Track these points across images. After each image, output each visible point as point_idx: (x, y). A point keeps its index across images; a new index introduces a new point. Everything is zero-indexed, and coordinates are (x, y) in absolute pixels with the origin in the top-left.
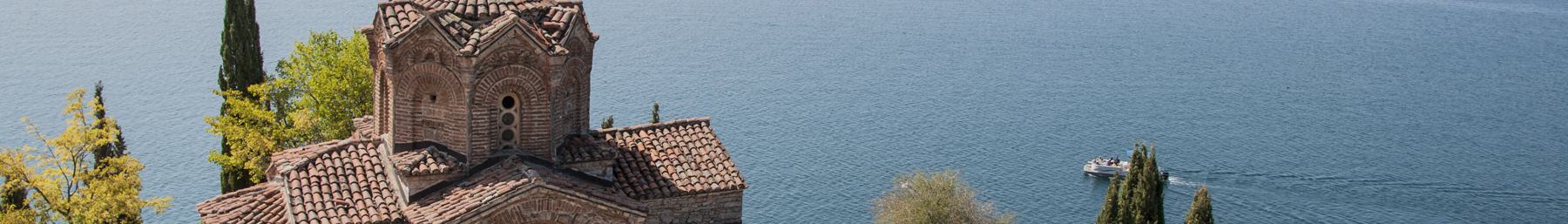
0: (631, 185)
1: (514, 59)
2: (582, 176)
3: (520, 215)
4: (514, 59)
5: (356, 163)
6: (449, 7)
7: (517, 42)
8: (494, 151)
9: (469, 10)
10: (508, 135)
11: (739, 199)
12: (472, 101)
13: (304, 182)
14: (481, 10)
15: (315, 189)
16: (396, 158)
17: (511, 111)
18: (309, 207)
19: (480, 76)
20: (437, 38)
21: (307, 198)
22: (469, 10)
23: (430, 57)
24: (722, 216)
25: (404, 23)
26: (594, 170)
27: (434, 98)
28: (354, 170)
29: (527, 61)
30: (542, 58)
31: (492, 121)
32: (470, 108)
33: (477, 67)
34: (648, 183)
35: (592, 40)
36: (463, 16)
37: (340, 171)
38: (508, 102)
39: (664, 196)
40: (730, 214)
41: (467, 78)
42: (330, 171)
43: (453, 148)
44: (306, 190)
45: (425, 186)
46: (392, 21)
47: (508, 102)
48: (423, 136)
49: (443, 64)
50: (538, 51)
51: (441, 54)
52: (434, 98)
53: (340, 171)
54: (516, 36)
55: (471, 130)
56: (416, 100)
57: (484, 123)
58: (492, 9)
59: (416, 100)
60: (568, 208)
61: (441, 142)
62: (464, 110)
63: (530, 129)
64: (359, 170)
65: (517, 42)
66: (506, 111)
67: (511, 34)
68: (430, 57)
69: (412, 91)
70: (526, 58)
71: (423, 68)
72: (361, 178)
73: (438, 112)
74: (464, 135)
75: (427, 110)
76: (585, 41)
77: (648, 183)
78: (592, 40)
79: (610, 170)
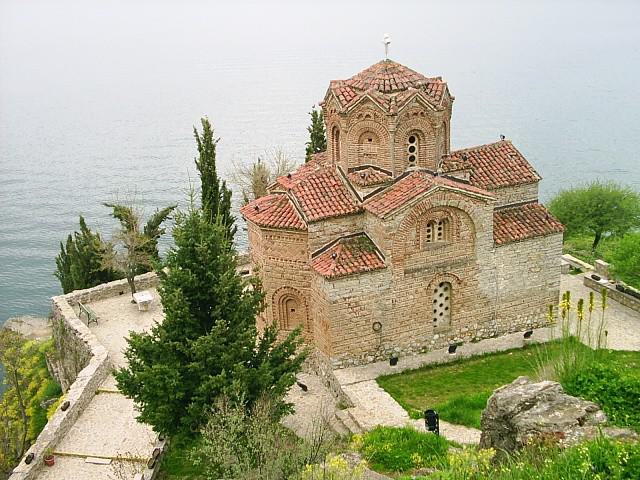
1: (416, 114)
6: (376, 87)
9: (387, 88)
10: (412, 159)
14: (394, 87)
17: (413, 145)
18: (311, 206)
22: (387, 88)
25: (349, 98)
26: (460, 176)
27: (370, 140)
36: (385, 92)
41: (392, 127)
42: (315, 185)
44: (305, 197)
45: (372, 191)
46: (342, 98)
47: (412, 140)
52: (370, 140)
56: (360, 142)
59: (360, 142)
62: (390, 147)
68: (368, 116)
74: (390, 160)
75: (367, 147)
79: (468, 175)
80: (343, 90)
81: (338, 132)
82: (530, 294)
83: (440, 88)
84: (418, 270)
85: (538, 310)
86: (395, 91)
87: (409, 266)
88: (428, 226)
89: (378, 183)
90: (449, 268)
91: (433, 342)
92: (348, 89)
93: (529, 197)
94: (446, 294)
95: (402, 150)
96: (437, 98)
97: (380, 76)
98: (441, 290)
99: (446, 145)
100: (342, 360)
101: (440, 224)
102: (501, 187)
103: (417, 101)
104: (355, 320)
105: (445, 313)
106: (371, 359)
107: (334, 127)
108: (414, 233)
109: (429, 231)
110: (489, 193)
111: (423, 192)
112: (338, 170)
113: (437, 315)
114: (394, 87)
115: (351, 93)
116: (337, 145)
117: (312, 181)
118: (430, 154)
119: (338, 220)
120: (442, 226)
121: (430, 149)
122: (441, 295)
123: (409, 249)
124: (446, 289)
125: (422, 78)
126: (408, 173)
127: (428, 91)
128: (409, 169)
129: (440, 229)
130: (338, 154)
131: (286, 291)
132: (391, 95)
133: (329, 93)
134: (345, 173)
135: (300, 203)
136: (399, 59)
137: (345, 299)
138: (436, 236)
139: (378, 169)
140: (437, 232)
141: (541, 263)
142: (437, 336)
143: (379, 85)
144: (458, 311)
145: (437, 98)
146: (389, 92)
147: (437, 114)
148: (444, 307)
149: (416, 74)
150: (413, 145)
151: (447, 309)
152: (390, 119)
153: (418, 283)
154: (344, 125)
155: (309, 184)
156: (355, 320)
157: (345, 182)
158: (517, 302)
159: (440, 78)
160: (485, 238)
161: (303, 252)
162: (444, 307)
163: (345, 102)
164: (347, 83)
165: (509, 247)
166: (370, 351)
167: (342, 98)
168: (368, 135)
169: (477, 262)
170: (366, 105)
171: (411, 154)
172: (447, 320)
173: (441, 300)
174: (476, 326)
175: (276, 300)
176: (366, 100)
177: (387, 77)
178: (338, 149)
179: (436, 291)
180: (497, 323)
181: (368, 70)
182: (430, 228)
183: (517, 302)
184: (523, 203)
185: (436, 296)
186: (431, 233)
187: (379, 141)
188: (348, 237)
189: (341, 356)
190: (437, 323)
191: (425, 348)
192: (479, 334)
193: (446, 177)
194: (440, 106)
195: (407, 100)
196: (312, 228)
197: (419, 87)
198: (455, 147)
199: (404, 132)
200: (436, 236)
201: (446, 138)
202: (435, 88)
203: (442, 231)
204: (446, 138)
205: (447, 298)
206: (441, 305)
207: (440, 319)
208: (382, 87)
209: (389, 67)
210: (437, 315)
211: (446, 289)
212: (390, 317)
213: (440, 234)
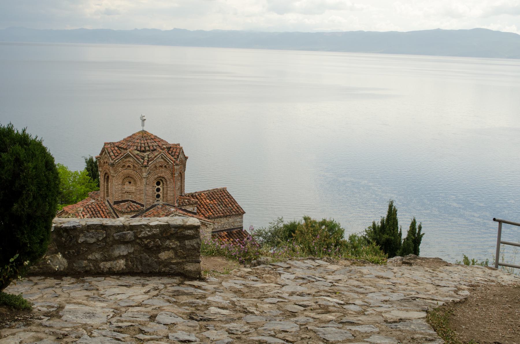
0: (202, 214)
1: (161, 166)
2: (185, 210)
4: (161, 166)
5: (99, 209)
6: (135, 148)
10: (158, 196)
11: (242, 218)
14: (147, 148)
16: (115, 206)
17: (159, 187)
20: (131, 160)
22: (143, 149)
24: (236, 224)
25: (116, 154)
26: (190, 209)
27: (130, 183)
28: (99, 212)
34: (208, 213)
35: (186, 158)
36: (140, 151)
37: (94, 212)
38: (158, 184)
40: (240, 224)
41: (145, 175)
46: (112, 154)
47: (158, 184)
49: (134, 170)
51: (134, 165)
53: (94, 212)
56: (123, 184)
58: (152, 148)
62: (143, 187)
63: (167, 194)
64: (101, 212)
65: (162, 160)
66: (157, 187)
68: (129, 166)
70: (165, 166)
71: (126, 171)
73: (131, 188)
75: (128, 187)
76: (184, 159)
77: (208, 213)
78: (186, 158)
79: (196, 208)
80: (113, 149)
81: (108, 177)
83: (178, 151)
86: (149, 151)
89: (134, 211)
92: (116, 148)
93: (237, 225)
95: (150, 190)
96: (176, 157)
97: (139, 141)
99: (182, 188)
102: (218, 217)
103: (162, 158)
107: (106, 174)
110: (209, 220)
112: (107, 203)
114: (147, 148)
115: (118, 151)
116: (107, 186)
117: (89, 210)
118: (170, 194)
121: (170, 191)
125: (167, 143)
126: (155, 205)
127: (170, 152)
128: (156, 203)
130: (107, 192)
132: (145, 154)
133: (103, 151)
134: (112, 204)
136: (152, 129)
143: (137, 147)
145: (176, 157)
146: (144, 151)
147: (176, 167)
149: (162, 140)
152: (143, 169)
154: (112, 172)
157: (112, 211)
159: (179, 145)
163: (114, 157)
164: (117, 144)
167: (112, 154)
168: (129, 179)
170: (128, 159)
171: (157, 193)
176: (128, 156)
177: (143, 142)
178: (107, 188)
181: (130, 137)
184: (232, 229)
187: (135, 183)
193: (181, 209)
194: (178, 162)
195: (155, 157)
197: (163, 149)
198: (189, 189)
199: (153, 178)
201: (181, 183)
202: (174, 151)
204: (181, 183)
208: (139, 148)
209: (144, 135)
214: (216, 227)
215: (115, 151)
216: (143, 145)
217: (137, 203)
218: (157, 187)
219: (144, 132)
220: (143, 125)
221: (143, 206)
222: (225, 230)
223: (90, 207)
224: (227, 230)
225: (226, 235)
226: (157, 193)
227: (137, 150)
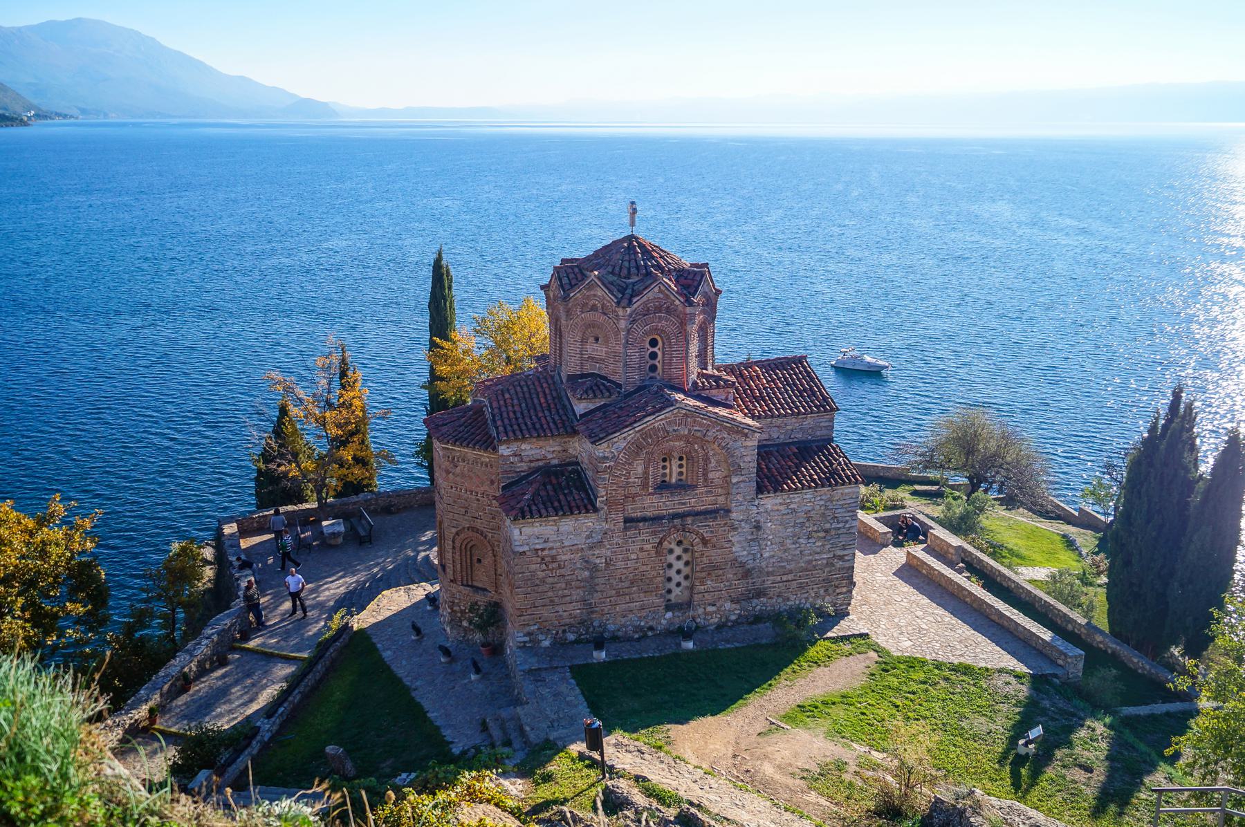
1: (658, 309)
3: (664, 429)
4: (658, 309)
7: (661, 296)
8: (643, 381)
9: (625, 272)
10: (653, 368)
12: (627, 342)
13: (502, 402)
15: (510, 408)
17: (655, 349)
19: (634, 321)
21: (505, 415)
23: (594, 308)
24: (818, 433)
27: (597, 339)
29: (668, 311)
30: (680, 308)
31: (642, 357)
32: (625, 347)
33: (630, 315)
35: (718, 292)
38: (654, 343)
39: (772, 417)
40: (824, 432)
41: (623, 324)
42: (521, 395)
43: (611, 378)
45: (592, 407)
47: (654, 343)
48: (588, 369)
50: (677, 302)
51: (603, 305)
52: (597, 339)
54: (660, 291)
55: (626, 365)
56: (584, 341)
57: (635, 359)
59: (584, 341)
60: (701, 425)
61: (603, 373)
62: (620, 349)
63: (670, 364)
64: (541, 395)
65: (661, 296)
66: (651, 350)
67: (656, 289)
69: (580, 334)
71: (589, 316)
72: (543, 400)
73: (600, 350)
75: (592, 348)
82: (810, 567)
84: (644, 519)
85: (822, 591)
87: (633, 510)
88: (664, 460)
90: (689, 520)
91: (663, 622)
94: (686, 557)
98: (678, 551)
100: (529, 634)
101: (681, 459)
104: (550, 580)
105: (685, 583)
106: (571, 637)
108: (640, 470)
109: (664, 468)
111: (653, 413)
113: (672, 585)
116: (561, 343)
117: (518, 389)
119: (541, 443)
120: (684, 462)
122: (679, 558)
123: (633, 490)
124: (686, 550)
126: (645, 387)
129: (681, 466)
131: (471, 534)
135: (494, 416)
137: (537, 550)
138: (674, 475)
139: (605, 378)
140: (675, 469)
141: (828, 526)
142: (669, 615)
144: (702, 583)
148: (682, 575)
150: (655, 349)
151: (686, 577)
153: (645, 539)
155: (512, 392)
156: (550, 580)
158: (790, 577)
160: (745, 483)
161: (492, 482)
162: (682, 575)
165: (779, 500)
166: (571, 625)
169: (734, 515)
171: (651, 362)
172: (687, 593)
173: (679, 565)
174: (728, 605)
175: (458, 544)
179: (671, 551)
180: (759, 605)
182: (667, 464)
183: (790, 577)
185: (671, 558)
186: (667, 471)
187: (607, 341)
188: (555, 466)
189: (527, 629)
190: (672, 596)
191: (651, 628)
192: (733, 618)
196: (504, 450)
200: (674, 475)
203: (684, 470)
205: (687, 563)
206: (679, 572)
207: (676, 591)
208: (617, 269)
210: (672, 585)
211: (686, 550)
212: (601, 581)
213: (681, 473)
214: (775, 435)
215: (571, 276)
216: (626, 264)
217: (610, 381)
218: (651, 350)
219: (631, 238)
220: (632, 224)
221: (620, 386)
222: (793, 443)
223: (523, 383)
224: (799, 442)
225: (794, 454)
226: (651, 362)
227: (612, 273)
